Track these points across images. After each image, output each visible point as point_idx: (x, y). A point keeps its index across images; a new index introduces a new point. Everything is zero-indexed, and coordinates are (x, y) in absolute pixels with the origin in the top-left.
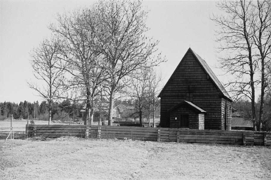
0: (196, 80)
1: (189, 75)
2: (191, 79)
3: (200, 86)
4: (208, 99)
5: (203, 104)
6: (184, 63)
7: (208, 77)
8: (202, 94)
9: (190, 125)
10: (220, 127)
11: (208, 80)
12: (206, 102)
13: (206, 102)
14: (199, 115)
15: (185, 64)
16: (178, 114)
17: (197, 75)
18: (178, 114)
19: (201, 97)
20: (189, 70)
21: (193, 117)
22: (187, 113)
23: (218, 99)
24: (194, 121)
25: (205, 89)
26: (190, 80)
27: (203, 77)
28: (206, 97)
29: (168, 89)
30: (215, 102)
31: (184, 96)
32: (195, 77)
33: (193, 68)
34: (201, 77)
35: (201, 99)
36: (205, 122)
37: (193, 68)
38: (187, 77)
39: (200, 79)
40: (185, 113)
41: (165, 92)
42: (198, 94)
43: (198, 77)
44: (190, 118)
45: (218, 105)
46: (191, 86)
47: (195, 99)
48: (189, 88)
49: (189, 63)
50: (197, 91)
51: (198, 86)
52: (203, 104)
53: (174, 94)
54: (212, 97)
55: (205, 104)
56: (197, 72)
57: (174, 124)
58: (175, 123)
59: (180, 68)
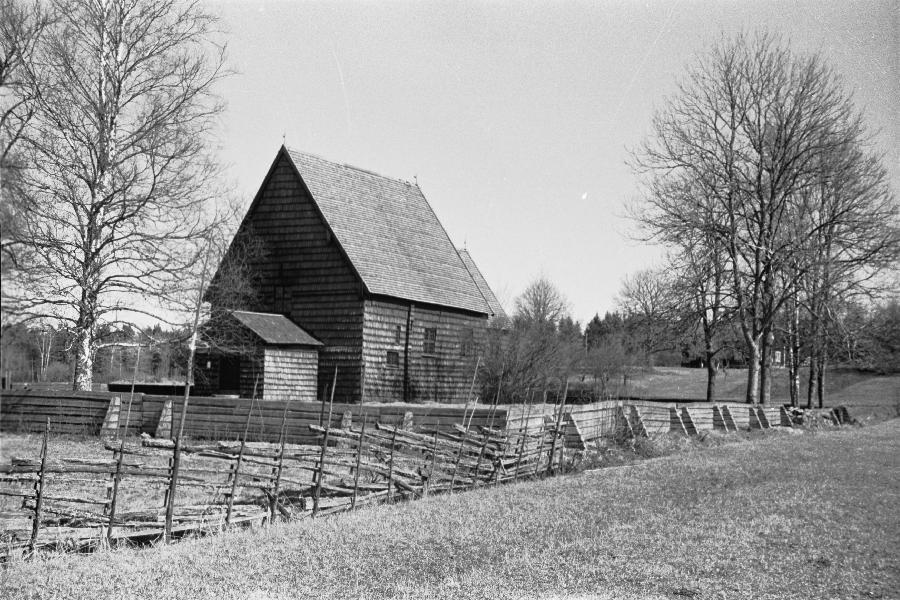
0: (300, 245)
1: (282, 231)
2: (286, 241)
4: (331, 305)
5: (315, 320)
6: (269, 194)
7: (328, 238)
8: (313, 288)
9: (243, 384)
10: (358, 391)
12: (323, 312)
13: (323, 312)
14: (267, 353)
15: (272, 197)
17: (302, 229)
19: (313, 299)
20: (283, 216)
23: (356, 304)
25: (322, 272)
26: (284, 246)
28: (324, 299)
30: (346, 312)
32: (298, 237)
33: (291, 208)
34: (311, 237)
35: (311, 306)
36: (318, 376)
37: (291, 208)
38: (276, 238)
39: (309, 244)
42: (305, 288)
43: (304, 237)
45: (354, 323)
46: (287, 266)
47: (296, 306)
48: (281, 270)
49: (283, 193)
50: (301, 281)
52: (315, 320)
54: (340, 298)
56: (302, 222)
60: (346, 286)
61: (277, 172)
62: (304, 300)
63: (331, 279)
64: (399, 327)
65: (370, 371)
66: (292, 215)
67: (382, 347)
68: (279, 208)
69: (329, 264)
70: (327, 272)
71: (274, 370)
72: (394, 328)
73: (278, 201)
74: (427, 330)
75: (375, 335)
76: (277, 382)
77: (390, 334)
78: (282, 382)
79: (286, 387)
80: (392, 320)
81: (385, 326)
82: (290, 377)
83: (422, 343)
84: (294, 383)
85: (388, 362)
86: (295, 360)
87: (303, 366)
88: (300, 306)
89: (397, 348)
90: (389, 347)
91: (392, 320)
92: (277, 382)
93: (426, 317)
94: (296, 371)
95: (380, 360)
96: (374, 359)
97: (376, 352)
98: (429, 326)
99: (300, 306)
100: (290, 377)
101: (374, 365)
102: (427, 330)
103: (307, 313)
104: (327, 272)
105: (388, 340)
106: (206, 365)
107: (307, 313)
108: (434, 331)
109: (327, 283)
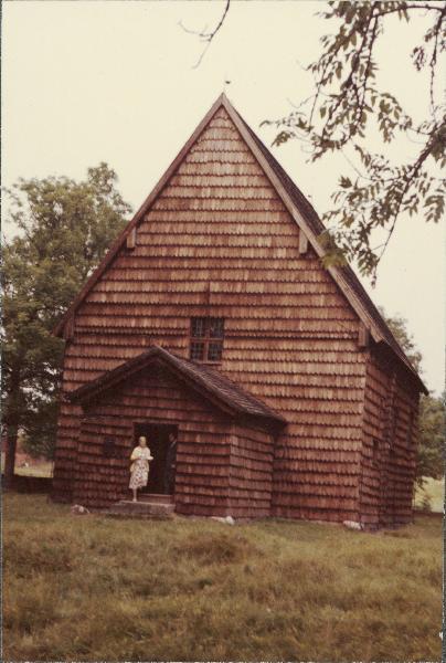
3: (261, 288)
6: (191, 169)
8: (265, 326)
9: (182, 484)
11: (303, 257)
16: (124, 423)
17: (250, 229)
18: (124, 423)
19: (262, 345)
20: (214, 205)
21: (198, 439)
22: (170, 415)
24: (206, 461)
25: (285, 301)
27: (279, 241)
28: (285, 345)
29: (103, 299)
31: (182, 336)
34: (268, 242)
35: (260, 356)
39: (262, 253)
40: (156, 419)
41: (88, 310)
44: (183, 443)
51: (251, 288)
52: (269, 379)
53: (133, 323)
54: (319, 346)
55: (282, 380)
57: (99, 478)
58: (102, 471)
59: (173, 192)
60: (331, 326)
61: (208, 135)
62: (250, 345)
63: (303, 313)
66: (233, 205)
68: (208, 192)
69: (301, 288)
73: (206, 181)
88: (238, 355)
99: (238, 355)
103: (254, 367)
107: (254, 367)
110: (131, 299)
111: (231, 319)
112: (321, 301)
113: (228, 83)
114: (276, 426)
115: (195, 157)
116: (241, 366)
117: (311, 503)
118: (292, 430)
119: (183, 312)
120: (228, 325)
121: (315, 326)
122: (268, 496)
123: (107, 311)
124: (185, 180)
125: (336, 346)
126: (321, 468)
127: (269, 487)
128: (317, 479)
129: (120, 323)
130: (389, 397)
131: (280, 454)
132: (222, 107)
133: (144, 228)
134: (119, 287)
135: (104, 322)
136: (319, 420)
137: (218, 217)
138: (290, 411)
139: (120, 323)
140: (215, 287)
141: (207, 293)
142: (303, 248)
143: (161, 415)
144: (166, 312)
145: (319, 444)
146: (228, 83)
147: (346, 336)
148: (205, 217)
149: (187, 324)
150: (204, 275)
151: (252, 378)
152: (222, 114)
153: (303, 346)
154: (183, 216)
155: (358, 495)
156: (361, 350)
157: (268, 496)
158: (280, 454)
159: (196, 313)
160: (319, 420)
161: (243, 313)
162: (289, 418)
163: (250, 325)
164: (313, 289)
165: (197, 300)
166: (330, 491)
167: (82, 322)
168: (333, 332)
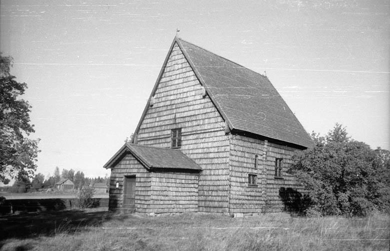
13: (202, 146)
16: (122, 175)
25: (200, 117)
40: (130, 173)
41: (140, 132)
55: (200, 151)
61: (172, 54)
63: (207, 121)
64: (256, 156)
65: (235, 188)
67: (244, 170)
70: (204, 117)
71: (159, 188)
72: (254, 156)
74: (277, 159)
75: (238, 161)
76: (163, 198)
77: (250, 161)
78: (167, 198)
79: (171, 202)
80: (252, 151)
81: (247, 155)
82: (174, 194)
83: (274, 168)
84: (178, 198)
85: (249, 182)
86: (178, 181)
87: (186, 185)
89: (255, 171)
90: (250, 171)
91: (252, 151)
92: (163, 198)
93: (276, 150)
94: (180, 189)
95: (243, 180)
96: (238, 180)
97: (239, 174)
98: (279, 156)
100: (174, 194)
101: (239, 184)
102: (277, 159)
104: (204, 117)
105: (249, 166)
106: (115, 185)
108: (281, 159)
109: (204, 124)
110: (153, 125)
111: (185, 127)
112: (211, 115)
113: (179, 31)
114: (197, 172)
115: (168, 65)
116: (187, 147)
117: (211, 204)
118: (204, 173)
119: (169, 127)
120: (183, 130)
121: (212, 126)
122: (197, 202)
123: (146, 131)
124: (167, 74)
125: (219, 134)
126: (215, 188)
127: (197, 198)
128: (214, 193)
129: (151, 135)
130: (264, 154)
131: (200, 183)
132: (176, 42)
133: (155, 97)
134: (149, 121)
135: (146, 135)
136: (214, 167)
137: (178, 87)
138: (202, 164)
139: (151, 135)
140: (178, 115)
141: (175, 119)
142: (204, 93)
143: (131, 171)
144: (163, 128)
145: (214, 178)
146: (179, 31)
147: (222, 129)
148: (173, 87)
149: (169, 132)
150: (174, 111)
151: (191, 152)
152: (176, 45)
153: (207, 135)
154: (168, 88)
155: (228, 199)
156: (227, 134)
157: (197, 202)
158: (200, 183)
159: (174, 127)
160: (214, 167)
161: (187, 125)
162: (203, 167)
163: (190, 130)
164: (209, 110)
165: (172, 122)
166: (219, 199)
167: (139, 137)
168: (217, 128)
